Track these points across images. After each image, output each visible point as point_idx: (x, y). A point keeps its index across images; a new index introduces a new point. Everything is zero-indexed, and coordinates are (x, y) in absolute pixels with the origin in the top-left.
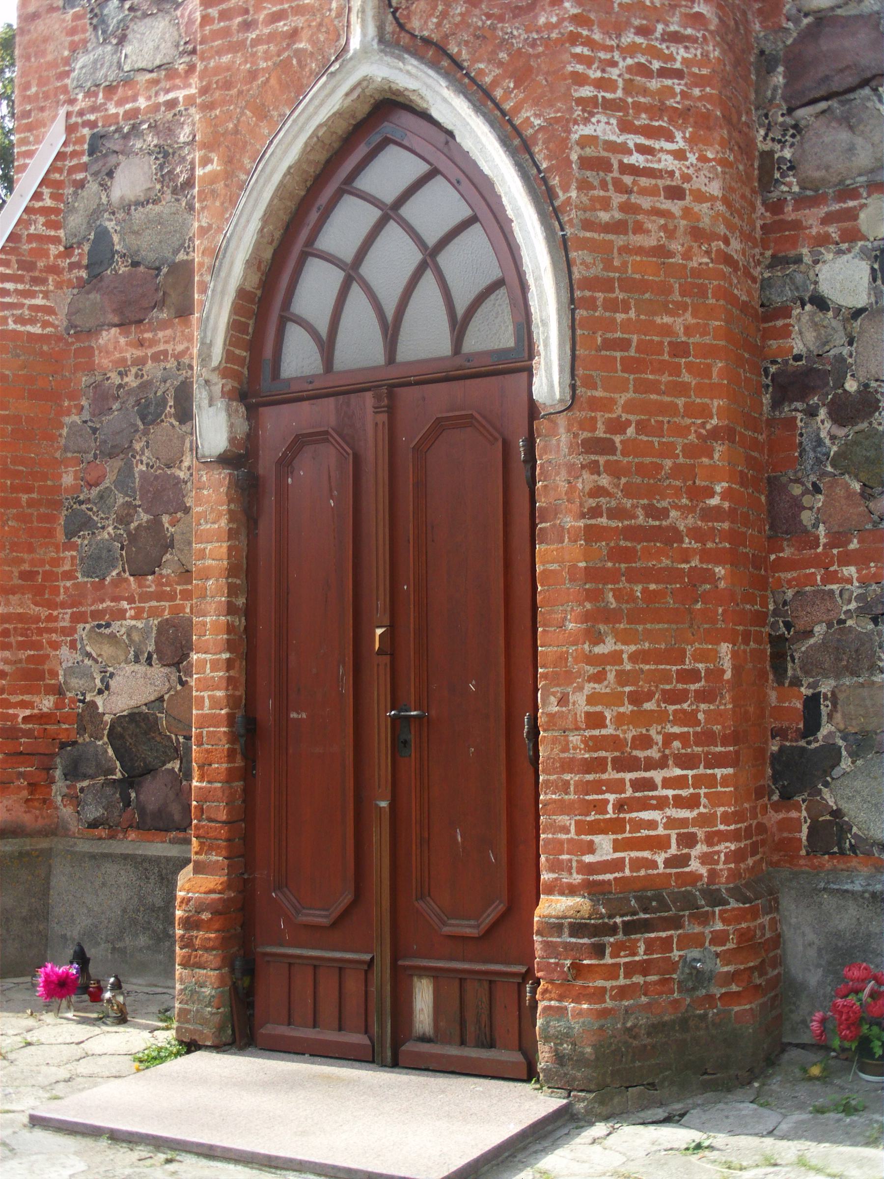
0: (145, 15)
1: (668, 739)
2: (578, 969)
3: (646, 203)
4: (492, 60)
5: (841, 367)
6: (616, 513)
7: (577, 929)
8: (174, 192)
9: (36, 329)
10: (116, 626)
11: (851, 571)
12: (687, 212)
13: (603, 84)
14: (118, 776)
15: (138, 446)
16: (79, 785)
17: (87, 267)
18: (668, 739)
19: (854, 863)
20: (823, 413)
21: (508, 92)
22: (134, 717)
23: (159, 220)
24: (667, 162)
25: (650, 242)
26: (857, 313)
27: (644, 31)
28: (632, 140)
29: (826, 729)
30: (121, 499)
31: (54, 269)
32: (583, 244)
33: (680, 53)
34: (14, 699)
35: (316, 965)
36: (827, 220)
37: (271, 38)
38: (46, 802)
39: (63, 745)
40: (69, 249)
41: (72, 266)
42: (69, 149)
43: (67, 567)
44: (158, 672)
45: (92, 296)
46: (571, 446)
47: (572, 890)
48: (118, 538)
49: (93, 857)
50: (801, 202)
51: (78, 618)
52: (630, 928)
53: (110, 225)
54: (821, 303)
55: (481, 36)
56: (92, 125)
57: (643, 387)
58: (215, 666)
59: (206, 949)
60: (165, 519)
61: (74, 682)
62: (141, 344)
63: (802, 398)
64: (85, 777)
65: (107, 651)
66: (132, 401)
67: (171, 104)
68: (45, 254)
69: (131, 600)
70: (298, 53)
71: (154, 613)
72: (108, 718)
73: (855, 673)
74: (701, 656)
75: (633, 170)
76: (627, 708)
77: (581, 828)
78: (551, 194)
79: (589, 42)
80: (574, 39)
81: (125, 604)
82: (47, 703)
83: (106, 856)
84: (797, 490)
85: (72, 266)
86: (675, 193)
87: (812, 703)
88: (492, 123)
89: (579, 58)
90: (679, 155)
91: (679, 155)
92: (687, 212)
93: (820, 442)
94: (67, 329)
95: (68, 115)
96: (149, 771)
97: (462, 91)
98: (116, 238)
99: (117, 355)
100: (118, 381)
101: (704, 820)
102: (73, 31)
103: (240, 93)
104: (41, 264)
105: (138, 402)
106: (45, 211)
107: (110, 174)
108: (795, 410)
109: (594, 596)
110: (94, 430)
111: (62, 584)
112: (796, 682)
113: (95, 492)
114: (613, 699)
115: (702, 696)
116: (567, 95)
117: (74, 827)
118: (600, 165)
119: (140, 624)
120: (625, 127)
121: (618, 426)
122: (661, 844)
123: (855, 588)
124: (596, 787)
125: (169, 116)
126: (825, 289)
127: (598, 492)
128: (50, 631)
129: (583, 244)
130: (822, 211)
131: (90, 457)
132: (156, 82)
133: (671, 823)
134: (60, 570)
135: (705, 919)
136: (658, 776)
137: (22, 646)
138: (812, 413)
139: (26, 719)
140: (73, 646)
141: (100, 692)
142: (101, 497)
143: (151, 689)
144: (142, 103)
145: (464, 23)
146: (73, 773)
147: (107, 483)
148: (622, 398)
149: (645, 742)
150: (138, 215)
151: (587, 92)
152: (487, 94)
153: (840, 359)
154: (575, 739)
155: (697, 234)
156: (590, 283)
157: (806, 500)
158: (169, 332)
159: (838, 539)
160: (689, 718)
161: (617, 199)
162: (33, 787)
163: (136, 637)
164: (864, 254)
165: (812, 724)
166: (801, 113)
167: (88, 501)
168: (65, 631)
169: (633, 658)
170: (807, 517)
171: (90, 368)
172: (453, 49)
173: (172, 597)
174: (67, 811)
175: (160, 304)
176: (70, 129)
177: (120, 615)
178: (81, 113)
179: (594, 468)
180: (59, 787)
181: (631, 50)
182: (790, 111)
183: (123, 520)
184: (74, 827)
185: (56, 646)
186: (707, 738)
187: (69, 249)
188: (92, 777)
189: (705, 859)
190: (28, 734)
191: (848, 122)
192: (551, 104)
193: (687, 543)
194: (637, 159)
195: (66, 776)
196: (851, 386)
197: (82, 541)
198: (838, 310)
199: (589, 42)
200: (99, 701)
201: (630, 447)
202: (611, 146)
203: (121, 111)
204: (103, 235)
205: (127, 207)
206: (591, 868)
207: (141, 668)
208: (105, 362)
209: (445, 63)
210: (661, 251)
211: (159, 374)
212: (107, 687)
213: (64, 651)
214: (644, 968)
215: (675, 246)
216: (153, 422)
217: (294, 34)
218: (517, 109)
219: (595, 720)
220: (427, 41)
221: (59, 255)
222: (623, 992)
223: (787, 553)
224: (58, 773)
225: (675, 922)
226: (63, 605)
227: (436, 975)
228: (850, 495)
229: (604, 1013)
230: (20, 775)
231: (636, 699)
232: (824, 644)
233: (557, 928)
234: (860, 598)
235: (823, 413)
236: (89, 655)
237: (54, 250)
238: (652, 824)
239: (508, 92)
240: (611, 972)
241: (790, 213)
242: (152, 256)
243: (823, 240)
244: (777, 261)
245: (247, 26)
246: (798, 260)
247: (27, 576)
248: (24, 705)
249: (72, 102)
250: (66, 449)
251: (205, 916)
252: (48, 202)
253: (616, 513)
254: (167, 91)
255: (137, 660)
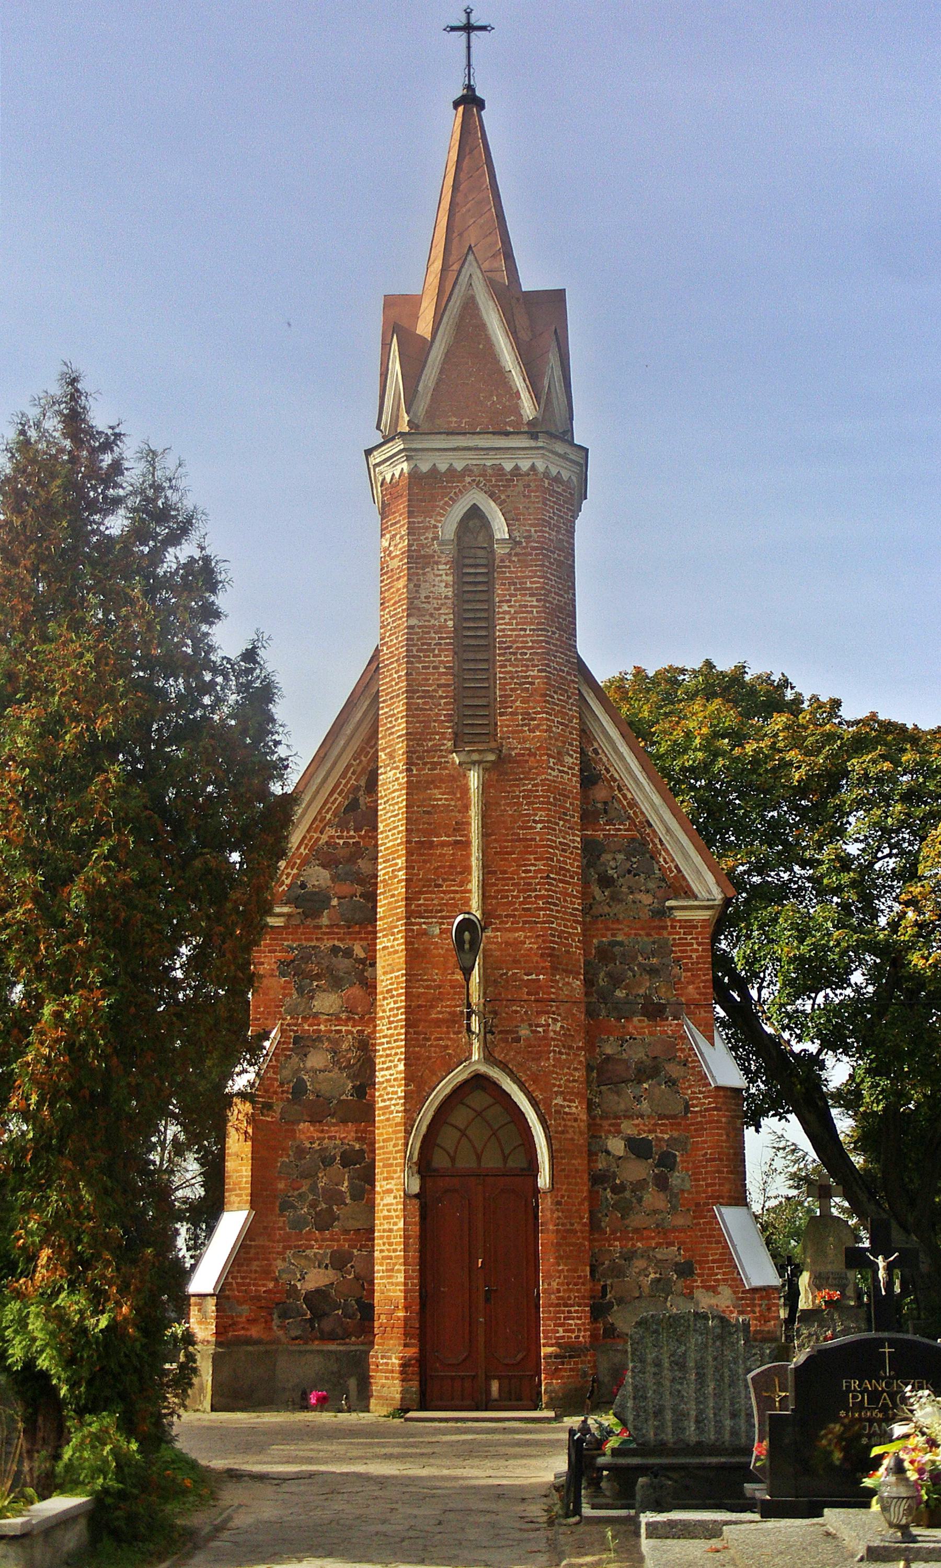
0: (324, 991)
1: (575, 1297)
2: (557, 1369)
3: (569, 1123)
4: (525, 1073)
5: (615, 1176)
6: (563, 1225)
7: (556, 1357)
8: (340, 1069)
9: (269, 1119)
10: (308, 1252)
11: (617, 1243)
12: (579, 1127)
13: (560, 1086)
14: (309, 1317)
15: (320, 1175)
16: (287, 1321)
17: (292, 1093)
18: (575, 1297)
19: (618, 1340)
20: (608, 1190)
21: (530, 1085)
22: (318, 1291)
23: (331, 1079)
24: (574, 1110)
25: (569, 1136)
26: (620, 1158)
27: (569, 1068)
28: (566, 1103)
29: (608, 1296)
30: (311, 1197)
31: (275, 1093)
32: (556, 1138)
33: (577, 1074)
34: (260, 1283)
35: (453, 1378)
36: (610, 1125)
37: (436, 1046)
38: (271, 1329)
39: (277, 1304)
40: (282, 1085)
41: (283, 1092)
42: (283, 1040)
43: (281, 1225)
44: (330, 1271)
45: (296, 1107)
46: (552, 1203)
47: (552, 1345)
48: (309, 1214)
49: (300, 1352)
50: (601, 1118)
51: (285, 1248)
52: (571, 1357)
53: (305, 1078)
54: (608, 1153)
55: (521, 1065)
56: (296, 1031)
57: (569, 1184)
58: (413, 1271)
59: (413, 1374)
60: (335, 1207)
61: (284, 1276)
62: (322, 1131)
63: (602, 1183)
64: (290, 1318)
65: (303, 1262)
66: (316, 1156)
67: (340, 1031)
68: (273, 1085)
69: (316, 1241)
70: (449, 1054)
71: (328, 1247)
72: (303, 1292)
73: (618, 1277)
74: (583, 1271)
75: (566, 1113)
76: (566, 1287)
77: (555, 1325)
78: (546, 1122)
79: (557, 1073)
80: (553, 1072)
81: (313, 1243)
82: (271, 1285)
83: (306, 1351)
84: (600, 1215)
85: (283, 1092)
86: (576, 1120)
87: (604, 1287)
88: (525, 1094)
89: (555, 1078)
90: (577, 1107)
91: (577, 1107)
92: (579, 1127)
93: (607, 1199)
94: (281, 1119)
95: (282, 1024)
96: (325, 1314)
97: (515, 1082)
98: (308, 1084)
99: (309, 1134)
100: (309, 1146)
101: (583, 1324)
102: (284, 988)
103: (424, 1063)
104: (271, 1090)
105: (320, 1156)
106: (273, 1067)
107: (305, 1055)
108: (599, 1188)
109: (558, 1251)
110: (297, 1166)
111: (277, 1232)
112: (599, 1280)
113: (296, 1193)
114: (562, 1284)
115: (583, 1284)
116: (551, 1090)
117: (284, 1339)
118: (558, 1112)
119: (321, 1251)
120: (565, 1100)
121: (563, 1196)
122: (572, 1331)
123: (618, 1249)
124: (558, 1312)
125: (337, 1036)
126: (610, 1148)
127: (559, 1218)
128: (273, 1253)
129: (556, 1138)
130: (609, 1122)
131: (295, 1177)
132: (331, 1021)
133: (576, 1325)
134: (276, 1226)
135: (586, 1356)
136: (573, 1309)
137: (264, 1259)
138: (605, 1189)
139: (264, 1292)
140: (284, 1260)
141: (299, 1280)
142: (300, 1195)
143: (327, 1279)
144: (322, 1027)
145: (514, 1058)
146: (284, 1315)
147: (303, 1189)
148: (564, 1187)
149: (569, 1298)
150: (321, 1076)
151: (556, 1089)
152: (523, 1084)
153: (614, 1172)
154: (553, 1296)
155: (581, 1133)
156: (557, 1151)
157: (603, 1219)
158: (336, 1128)
159: (613, 1232)
160: (578, 1291)
161: (563, 1123)
162: (266, 1322)
163: (318, 1256)
164: (622, 1139)
165: (604, 1294)
166: (602, 1087)
167: (293, 1196)
168: (278, 1253)
169: (568, 1271)
170: (603, 1224)
171: (294, 1139)
172: (510, 1066)
173: (338, 1241)
174: (280, 1333)
175: (332, 1115)
176: (282, 1031)
177: (312, 1247)
178: (288, 1025)
179: (557, 1210)
180: (276, 1321)
181: (565, 1075)
182: (599, 1086)
183: (313, 1205)
184: (284, 1339)
185: (275, 1259)
186: (583, 1297)
187: (282, 1085)
188: (293, 1318)
189: (583, 1337)
190: (265, 1298)
191: (618, 1093)
192: (546, 1092)
193: (579, 1234)
194: (567, 1110)
195: (279, 1317)
196: (618, 1181)
197: (289, 1213)
198: (614, 1156)
199: (557, 1073)
200: (299, 1285)
201: (567, 1204)
202: (562, 1106)
203: (311, 1029)
204: (301, 1081)
205: (315, 1071)
206: (558, 1338)
207: (322, 1271)
208: (302, 1137)
209: (507, 1070)
210: (573, 1139)
211: (332, 1146)
212: (304, 1278)
213: (279, 1262)
214: (571, 1370)
215: (576, 1137)
216: (329, 1165)
217: (447, 1047)
218: (533, 1091)
219: (558, 1291)
220: (501, 1062)
221: (278, 1086)
222: (569, 1377)
223: (596, 1236)
224: (275, 1316)
225: (579, 1356)
226: (278, 1241)
227: (499, 1378)
228: (617, 1217)
229: (564, 1383)
230: (262, 1317)
231: (568, 1284)
232: (609, 1267)
233: (550, 1357)
234: (620, 1252)
235: (608, 1190)
236: (293, 1264)
237: (276, 1084)
238: (571, 1325)
239: (530, 1085)
240: (565, 1370)
241: (598, 1121)
242: (328, 1094)
243: (610, 1131)
244: (593, 1137)
245: (428, 1039)
246: (601, 1137)
247: (265, 1228)
248: (264, 1285)
249: (284, 1019)
250: (280, 1172)
251: (413, 1362)
252: (274, 1063)
253: (563, 1225)
254: (336, 1026)
255: (319, 1267)
